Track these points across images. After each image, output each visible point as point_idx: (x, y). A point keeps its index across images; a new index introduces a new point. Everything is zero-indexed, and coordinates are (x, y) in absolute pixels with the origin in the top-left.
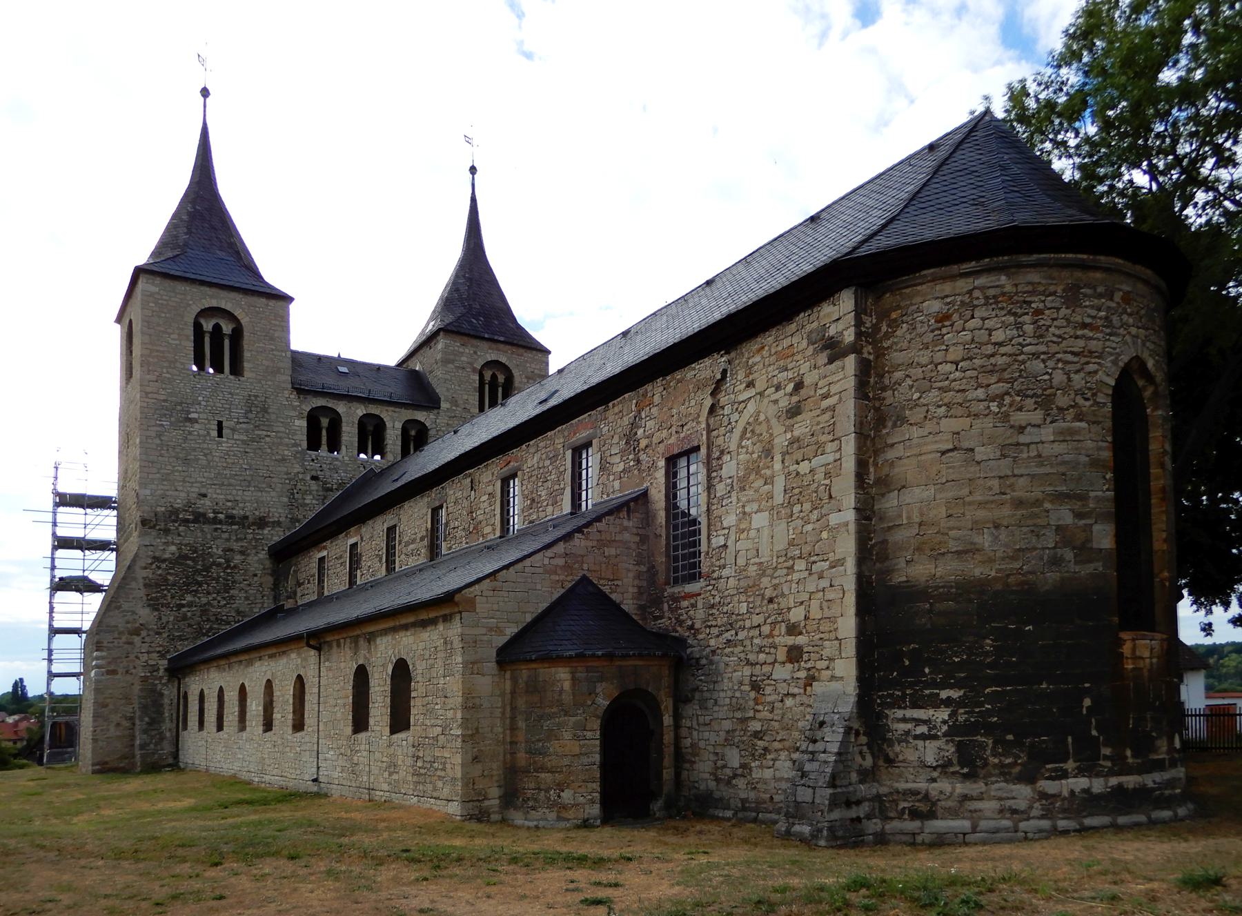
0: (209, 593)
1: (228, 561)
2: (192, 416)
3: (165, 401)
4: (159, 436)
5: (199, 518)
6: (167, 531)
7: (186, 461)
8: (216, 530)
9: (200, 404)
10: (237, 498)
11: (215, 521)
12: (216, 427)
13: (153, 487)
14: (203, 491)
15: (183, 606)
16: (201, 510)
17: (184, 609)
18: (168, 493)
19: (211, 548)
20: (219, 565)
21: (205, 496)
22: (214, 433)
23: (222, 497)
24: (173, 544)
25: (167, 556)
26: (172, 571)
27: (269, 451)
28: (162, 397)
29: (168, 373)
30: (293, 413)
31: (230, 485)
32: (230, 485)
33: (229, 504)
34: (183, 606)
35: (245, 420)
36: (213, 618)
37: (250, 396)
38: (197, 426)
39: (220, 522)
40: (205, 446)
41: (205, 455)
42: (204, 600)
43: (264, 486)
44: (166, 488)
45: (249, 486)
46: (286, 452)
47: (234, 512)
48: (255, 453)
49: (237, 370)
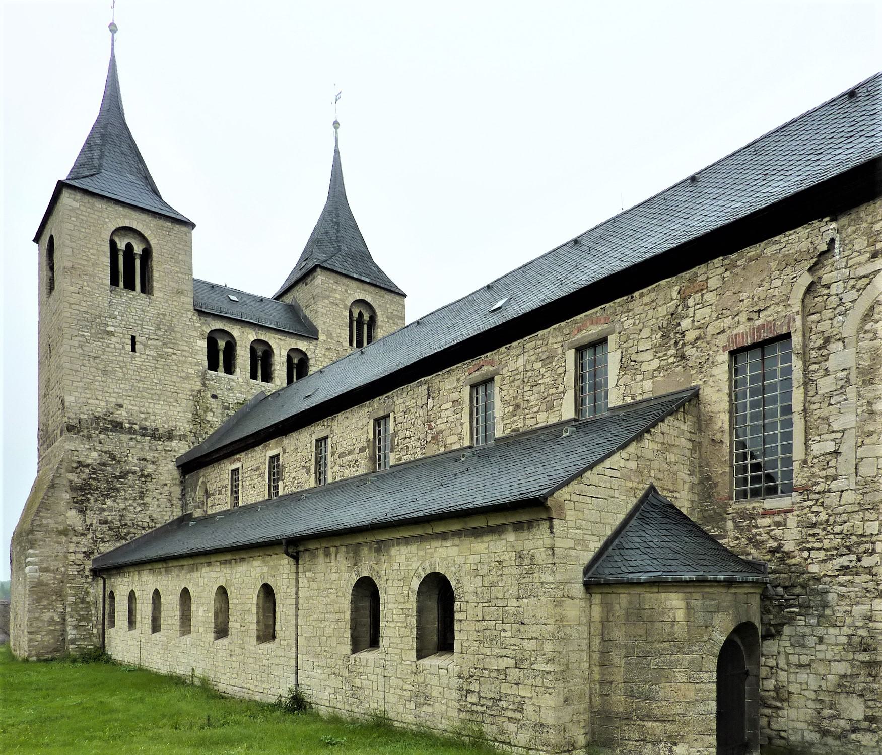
0: (126, 499)
1: (141, 471)
2: (109, 329)
3: (86, 312)
4: (81, 346)
5: (117, 426)
6: (89, 437)
7: (105, 372)
8: (131, 439)
9: (115, 318)
10: (150, 411)
11: (131, 431)
12: (130, 342)
13: (76, 394)
14: (120, 401)
15: (104, 510)
16: (118, 420)
17: (106, 513)
18: (90, 401)
19: (127, 456)
20: (134, 473)
21: (121, 406)
22: (129, 347)
23: (136, 408)
24: (95, 450)
25: (89, 462)
26: (94, 476)
27: (175, 368)
28: (85, 309)
29: (88, 286)
30: (195, 334)
31: (143, 397)
32: (143, 397)
33: (143, 416)
34: (104, 510)
35: (156, 337)
36: (130, 523)
37: (158, 314)
38: (114, 339)
39: (135, 432)
40: (121, 359)
41: (121, 368)
42: (122, 506)
43: (172, 400)
44: (88, 396)
45: (159, 400)
46: (190, 371)
47: (147, 423)
48: (164, 369)
49: (146, 288)
